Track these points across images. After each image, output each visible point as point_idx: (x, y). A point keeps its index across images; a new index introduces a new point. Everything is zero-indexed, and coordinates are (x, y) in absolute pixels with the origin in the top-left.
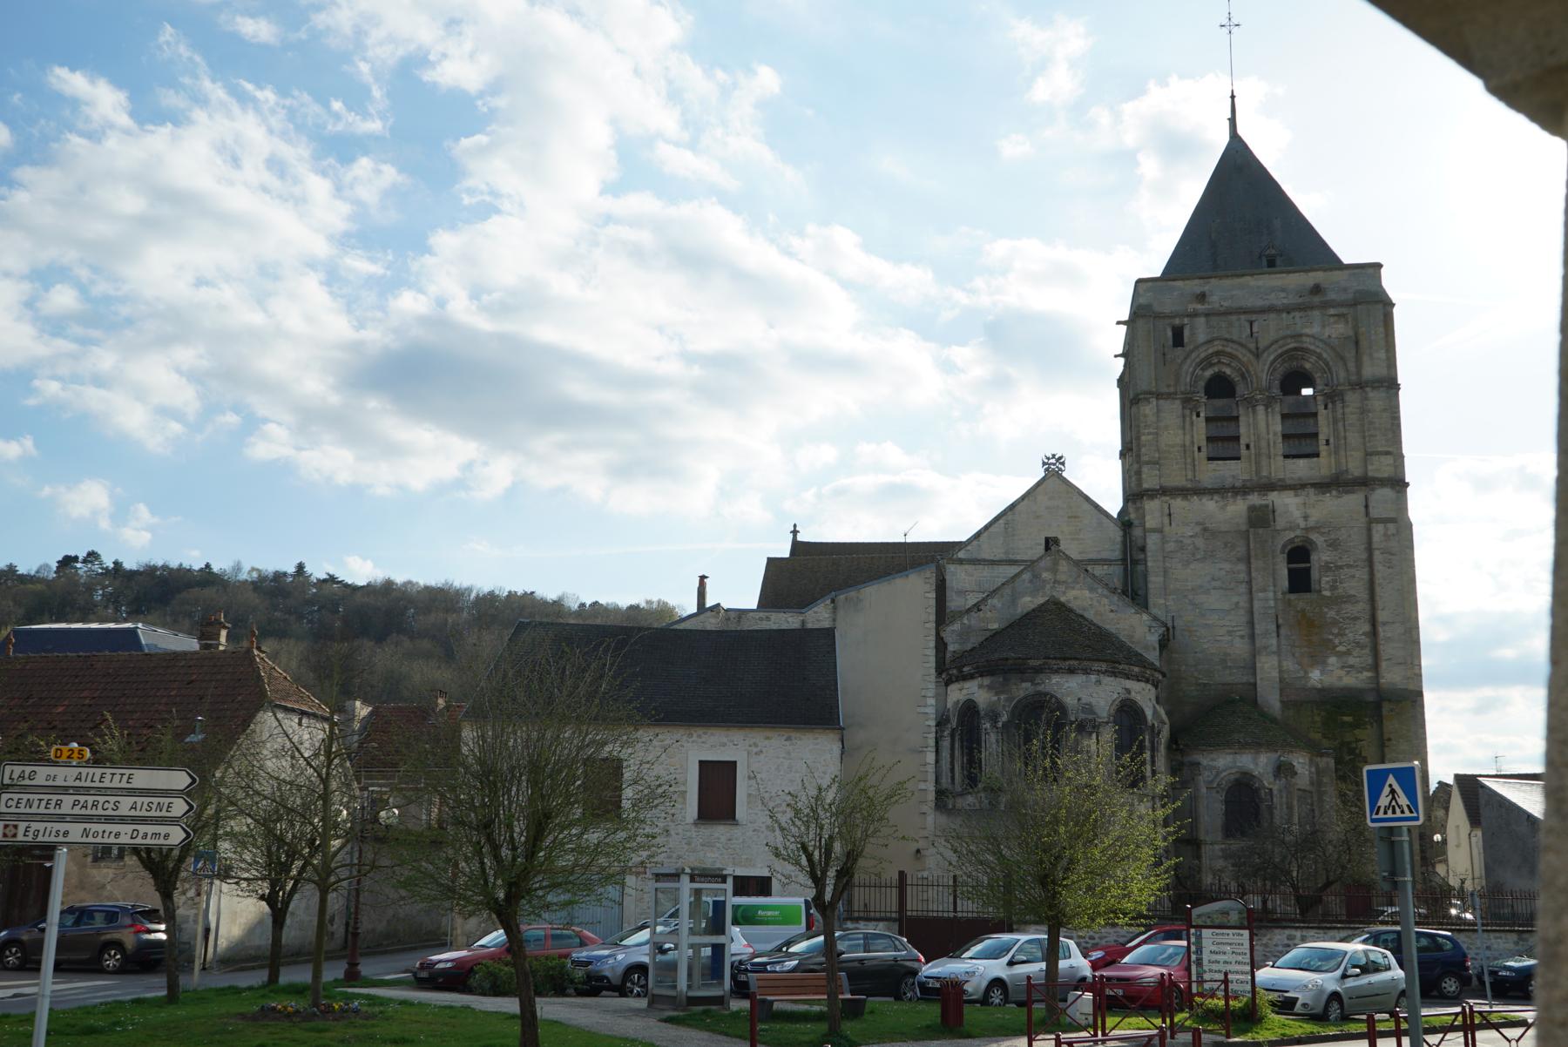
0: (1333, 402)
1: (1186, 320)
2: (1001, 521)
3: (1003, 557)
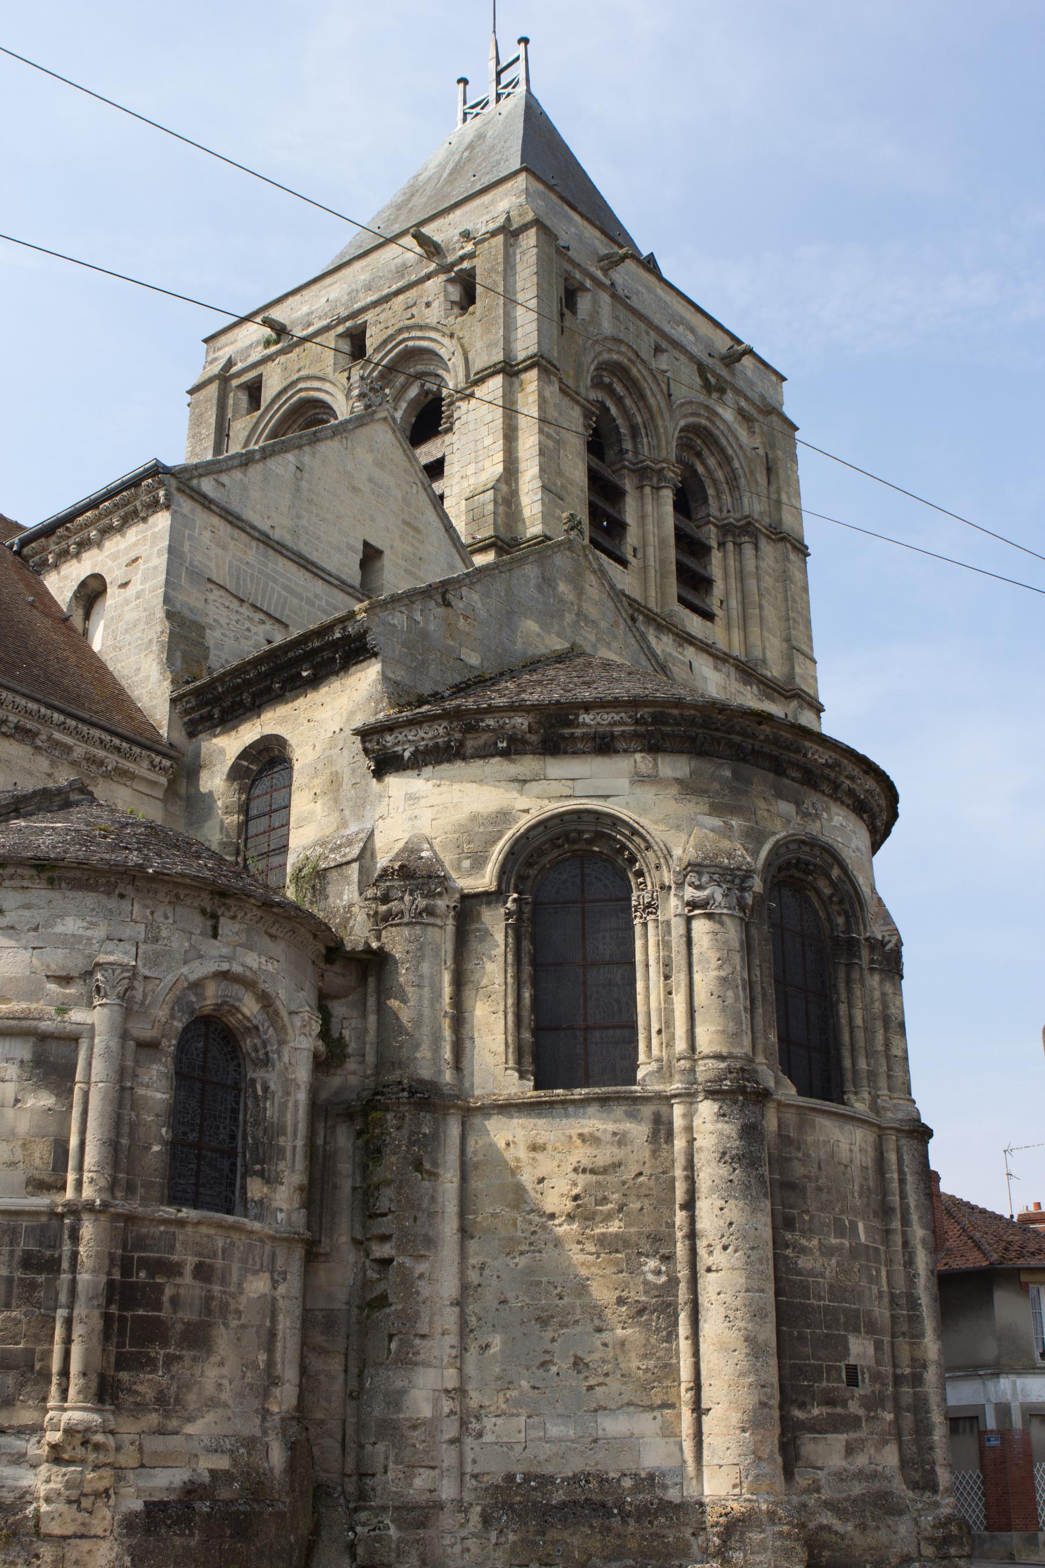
0: (738, 545)
1: (588, 283)
2: (290, 457)
3: (288, 540)
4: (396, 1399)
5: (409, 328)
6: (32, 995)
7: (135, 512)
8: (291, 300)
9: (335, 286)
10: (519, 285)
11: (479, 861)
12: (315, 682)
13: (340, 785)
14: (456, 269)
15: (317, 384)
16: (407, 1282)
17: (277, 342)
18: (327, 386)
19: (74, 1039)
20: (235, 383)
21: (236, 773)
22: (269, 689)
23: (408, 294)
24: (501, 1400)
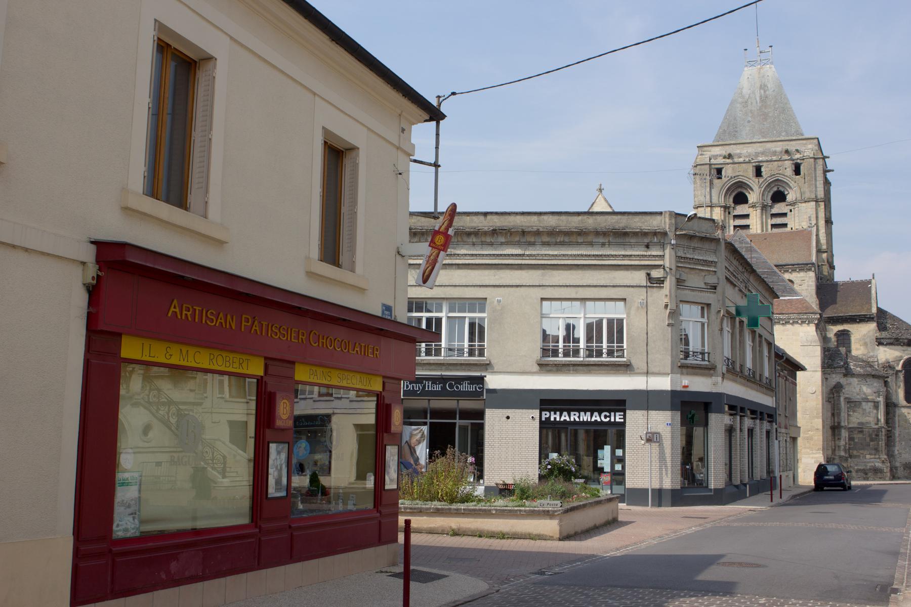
4: (893, 451)
5: (779, 174)
6: (872, 396)
7: (803, 270)
8: (732, 146)
9: (750, 148)
10: (817, 175)
11: (898, 365)
12: (858, 322)
13: (867, 345)
14: (795, 161)
15: (748, 180)
16: (894, 434)
17: (728, 159)
18: (751, 181)
19: (878, 402)
20: (713, 166)
21: (836, 334)
22: (847, 321)
23: (778, 162)
24: (904, 452)
